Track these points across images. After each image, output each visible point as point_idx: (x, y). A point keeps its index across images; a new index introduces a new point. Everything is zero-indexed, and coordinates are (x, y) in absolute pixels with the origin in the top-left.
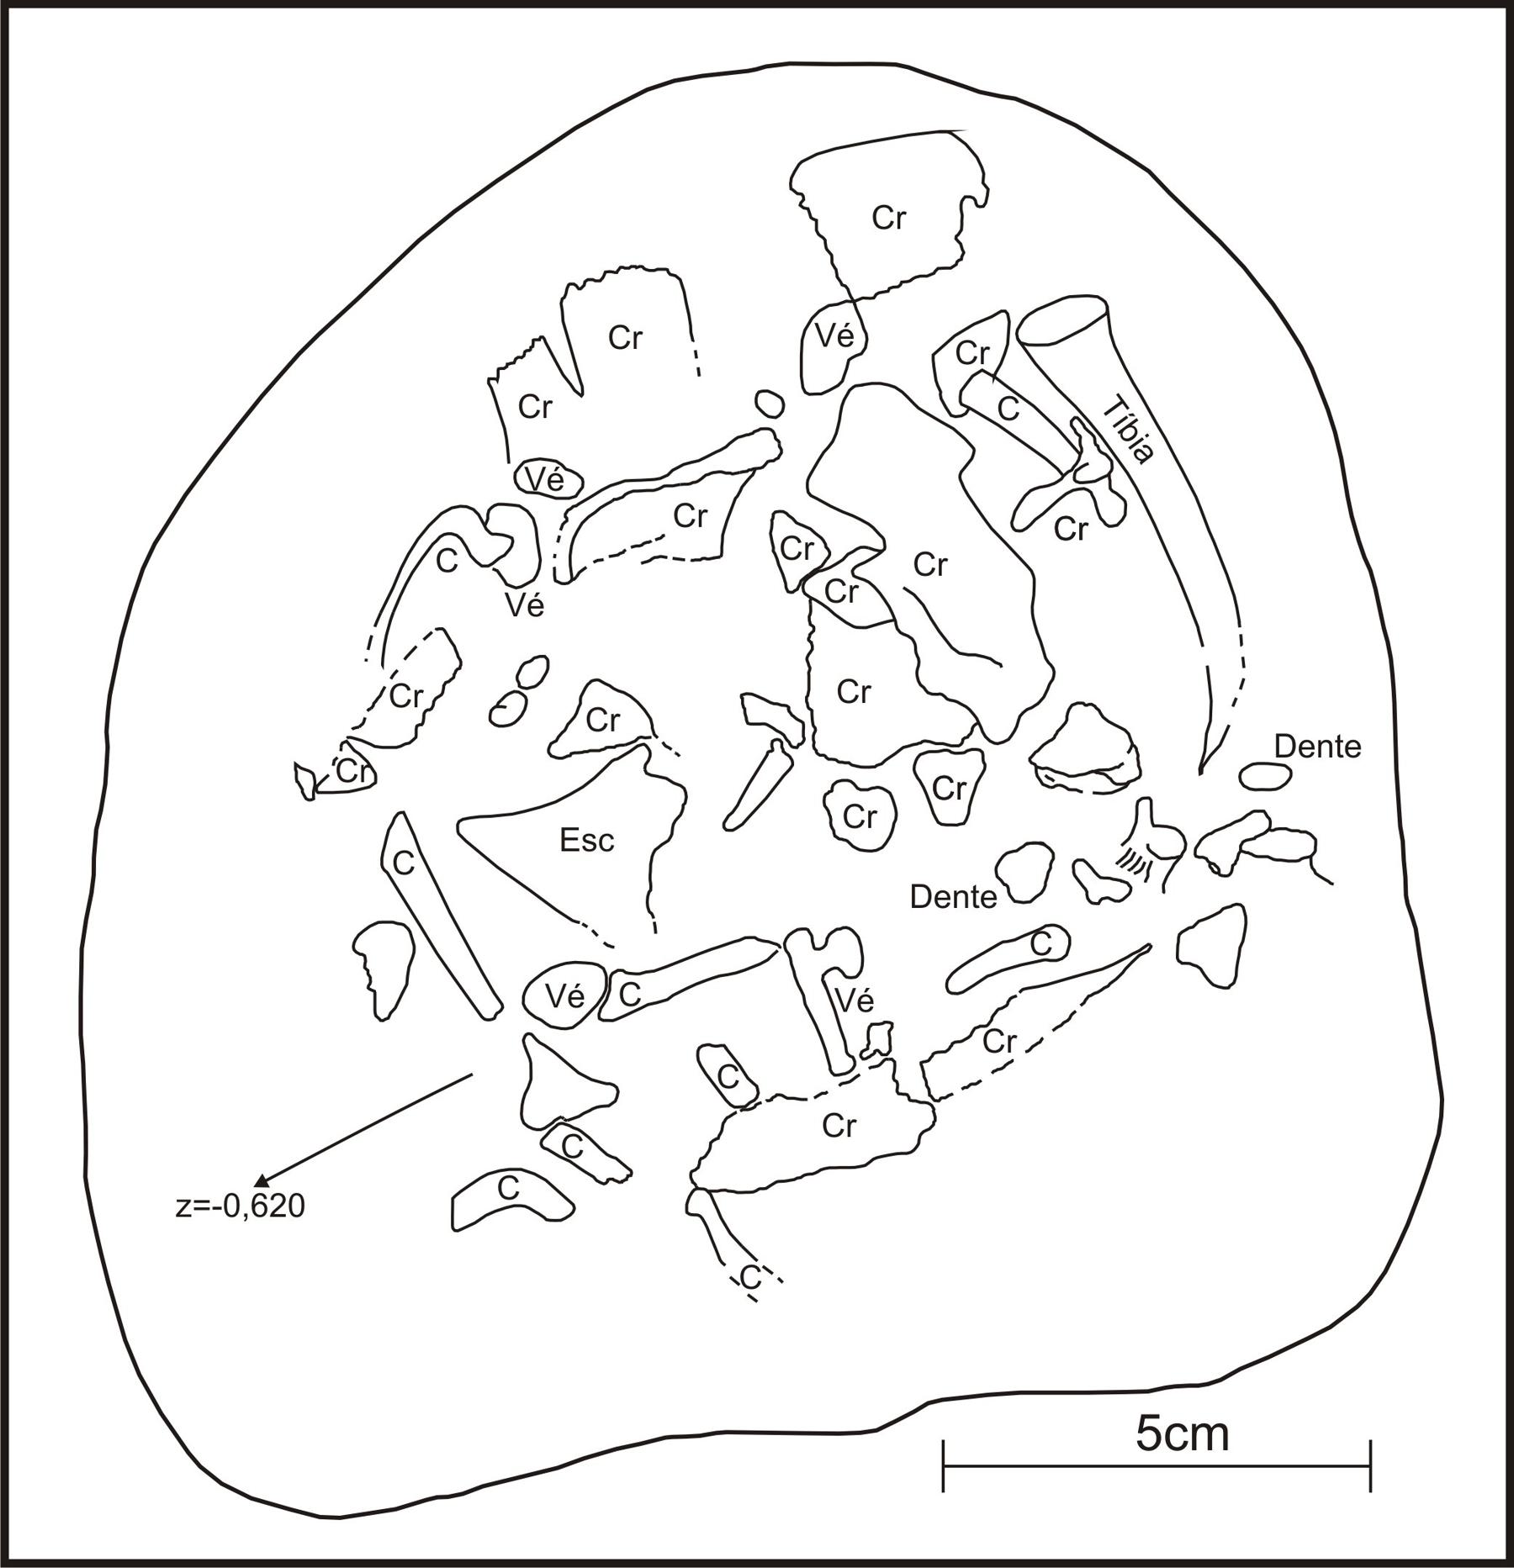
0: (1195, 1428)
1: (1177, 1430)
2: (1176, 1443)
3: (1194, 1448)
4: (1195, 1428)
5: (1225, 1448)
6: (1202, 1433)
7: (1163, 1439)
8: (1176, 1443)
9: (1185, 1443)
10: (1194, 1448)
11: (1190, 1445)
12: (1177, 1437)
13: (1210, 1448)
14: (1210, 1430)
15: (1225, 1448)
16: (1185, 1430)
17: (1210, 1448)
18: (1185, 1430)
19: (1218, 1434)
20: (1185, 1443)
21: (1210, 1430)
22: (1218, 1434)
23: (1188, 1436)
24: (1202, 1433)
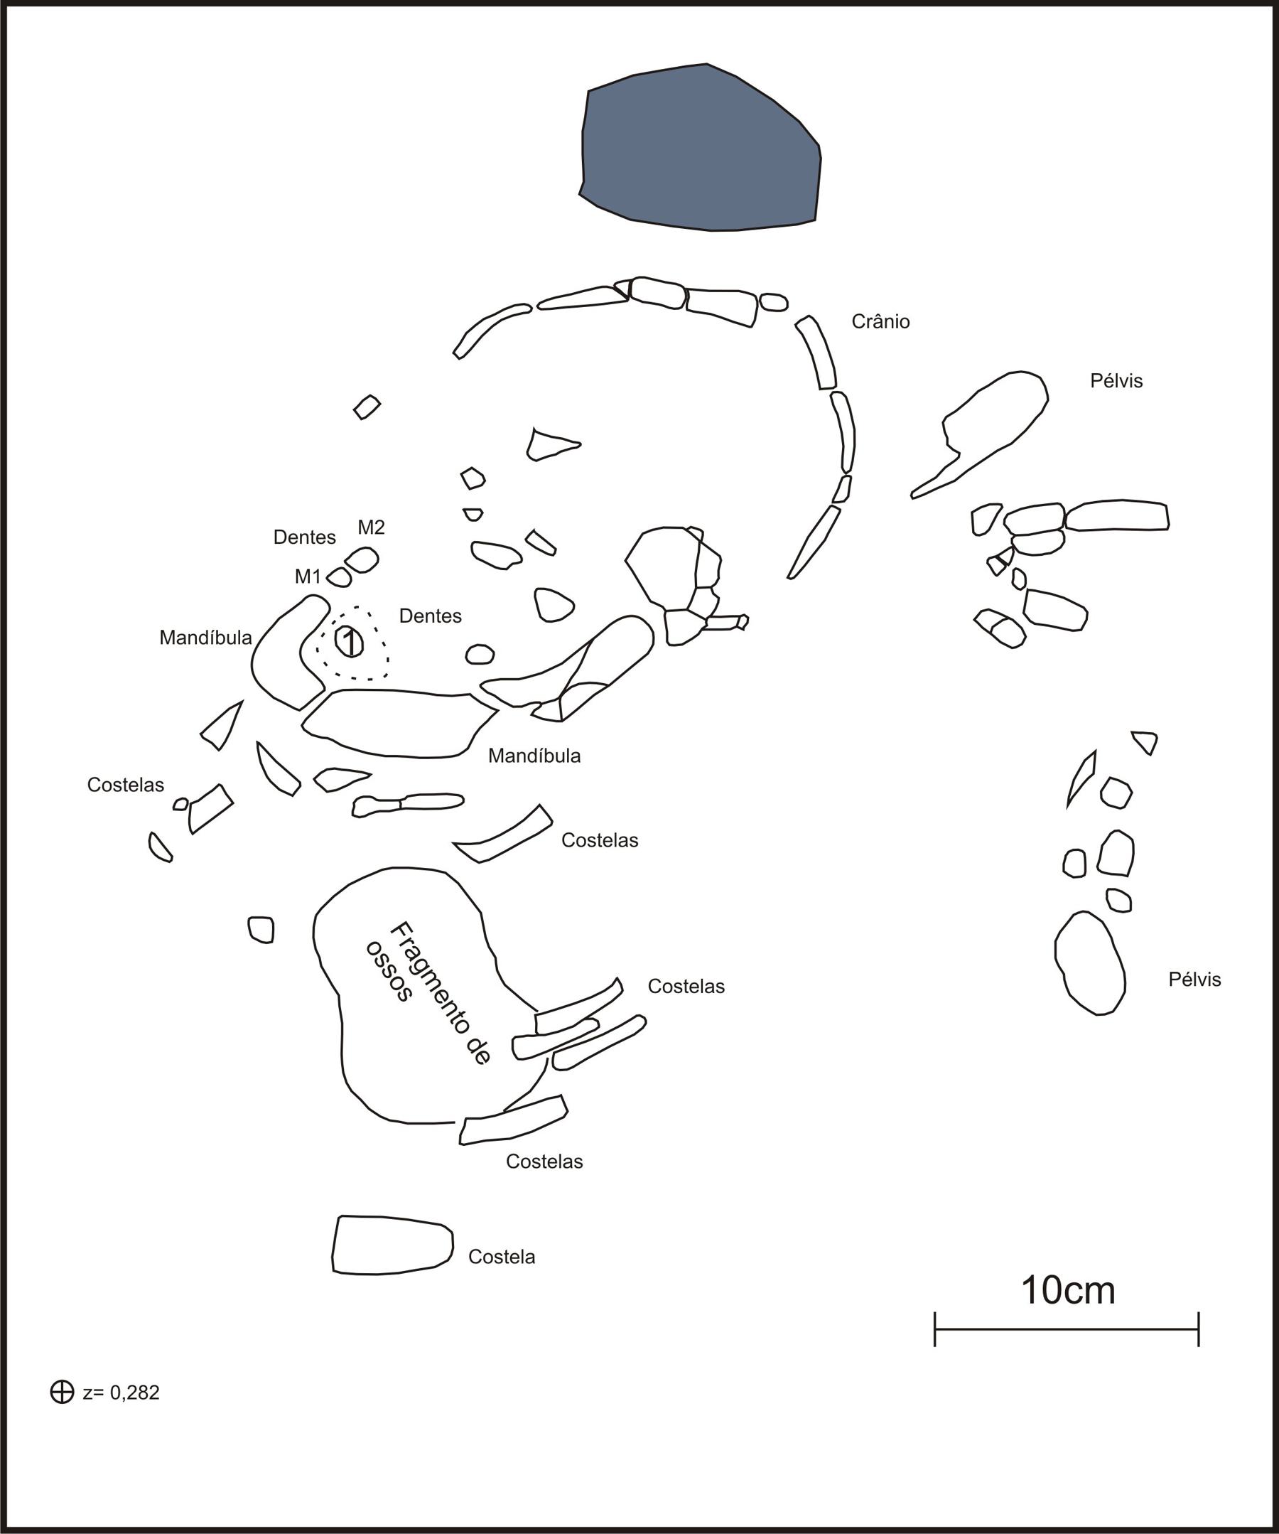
0: (1088, 1286)
1: (1073, 1289)
2: (1073, 1297)
3: (1088, 1301)
4: (1088, 1286)
5: (1112, 1301)
6: (1094, 1290)
7: (1064, 1292)
8: (1073, 1297)
9: (1081, 1298)
10: (1088, 1301)
11: (1084, 1299)
12: (1075, 1293)
13: (1100, 1301)
14: (1100, 1287)
15: (1112, 1301)
16: (1080, 1287)
17: (1100, 1301)
18: (1080, 1287)
19: (1106, 1290)
20: (1081, 1298)
21: (1100, 1287)
22: (1106, 1290)
23: (1083, 1293)
24: (1094, 1290)
